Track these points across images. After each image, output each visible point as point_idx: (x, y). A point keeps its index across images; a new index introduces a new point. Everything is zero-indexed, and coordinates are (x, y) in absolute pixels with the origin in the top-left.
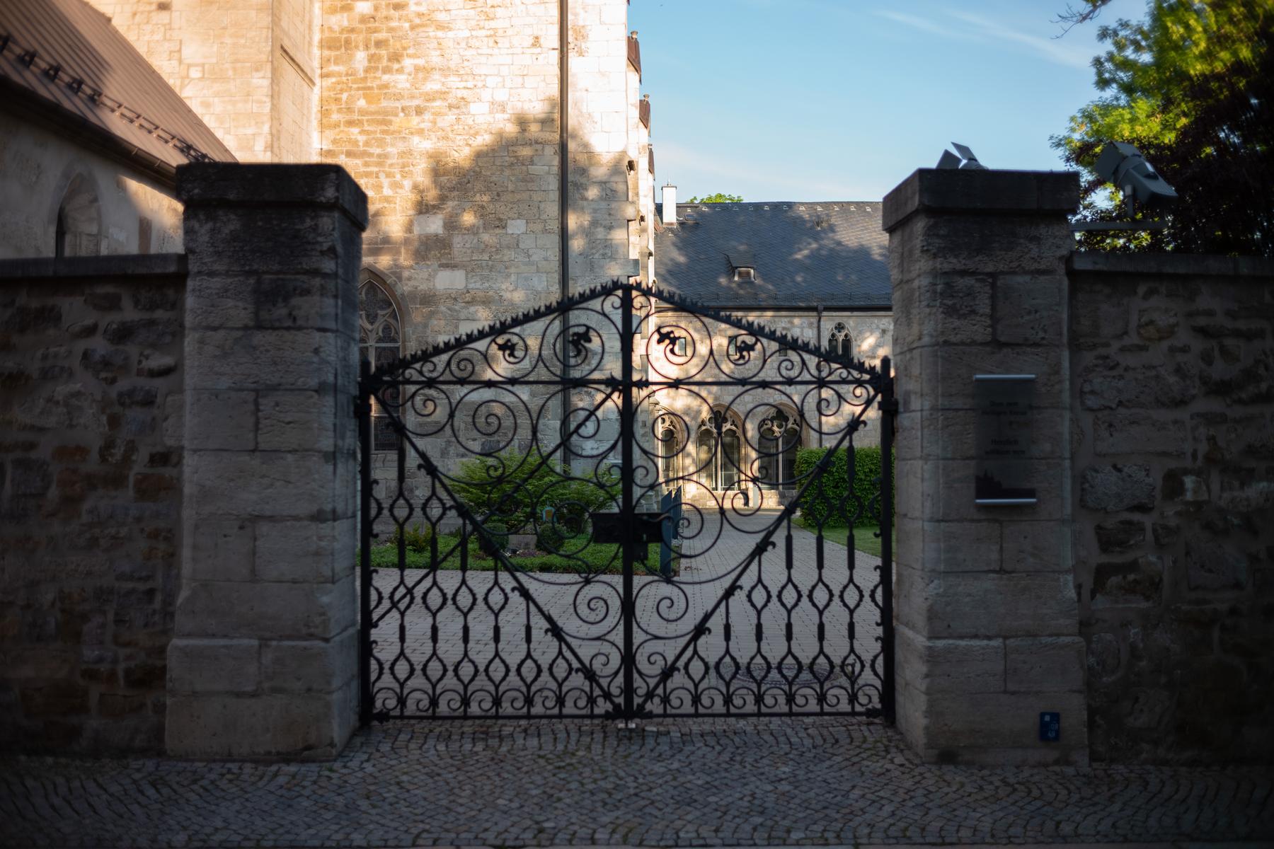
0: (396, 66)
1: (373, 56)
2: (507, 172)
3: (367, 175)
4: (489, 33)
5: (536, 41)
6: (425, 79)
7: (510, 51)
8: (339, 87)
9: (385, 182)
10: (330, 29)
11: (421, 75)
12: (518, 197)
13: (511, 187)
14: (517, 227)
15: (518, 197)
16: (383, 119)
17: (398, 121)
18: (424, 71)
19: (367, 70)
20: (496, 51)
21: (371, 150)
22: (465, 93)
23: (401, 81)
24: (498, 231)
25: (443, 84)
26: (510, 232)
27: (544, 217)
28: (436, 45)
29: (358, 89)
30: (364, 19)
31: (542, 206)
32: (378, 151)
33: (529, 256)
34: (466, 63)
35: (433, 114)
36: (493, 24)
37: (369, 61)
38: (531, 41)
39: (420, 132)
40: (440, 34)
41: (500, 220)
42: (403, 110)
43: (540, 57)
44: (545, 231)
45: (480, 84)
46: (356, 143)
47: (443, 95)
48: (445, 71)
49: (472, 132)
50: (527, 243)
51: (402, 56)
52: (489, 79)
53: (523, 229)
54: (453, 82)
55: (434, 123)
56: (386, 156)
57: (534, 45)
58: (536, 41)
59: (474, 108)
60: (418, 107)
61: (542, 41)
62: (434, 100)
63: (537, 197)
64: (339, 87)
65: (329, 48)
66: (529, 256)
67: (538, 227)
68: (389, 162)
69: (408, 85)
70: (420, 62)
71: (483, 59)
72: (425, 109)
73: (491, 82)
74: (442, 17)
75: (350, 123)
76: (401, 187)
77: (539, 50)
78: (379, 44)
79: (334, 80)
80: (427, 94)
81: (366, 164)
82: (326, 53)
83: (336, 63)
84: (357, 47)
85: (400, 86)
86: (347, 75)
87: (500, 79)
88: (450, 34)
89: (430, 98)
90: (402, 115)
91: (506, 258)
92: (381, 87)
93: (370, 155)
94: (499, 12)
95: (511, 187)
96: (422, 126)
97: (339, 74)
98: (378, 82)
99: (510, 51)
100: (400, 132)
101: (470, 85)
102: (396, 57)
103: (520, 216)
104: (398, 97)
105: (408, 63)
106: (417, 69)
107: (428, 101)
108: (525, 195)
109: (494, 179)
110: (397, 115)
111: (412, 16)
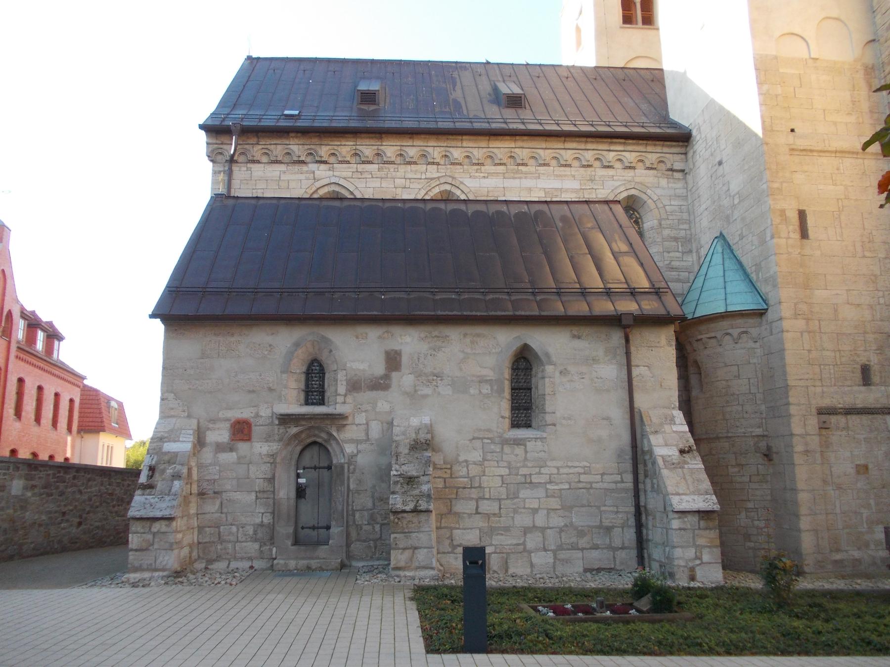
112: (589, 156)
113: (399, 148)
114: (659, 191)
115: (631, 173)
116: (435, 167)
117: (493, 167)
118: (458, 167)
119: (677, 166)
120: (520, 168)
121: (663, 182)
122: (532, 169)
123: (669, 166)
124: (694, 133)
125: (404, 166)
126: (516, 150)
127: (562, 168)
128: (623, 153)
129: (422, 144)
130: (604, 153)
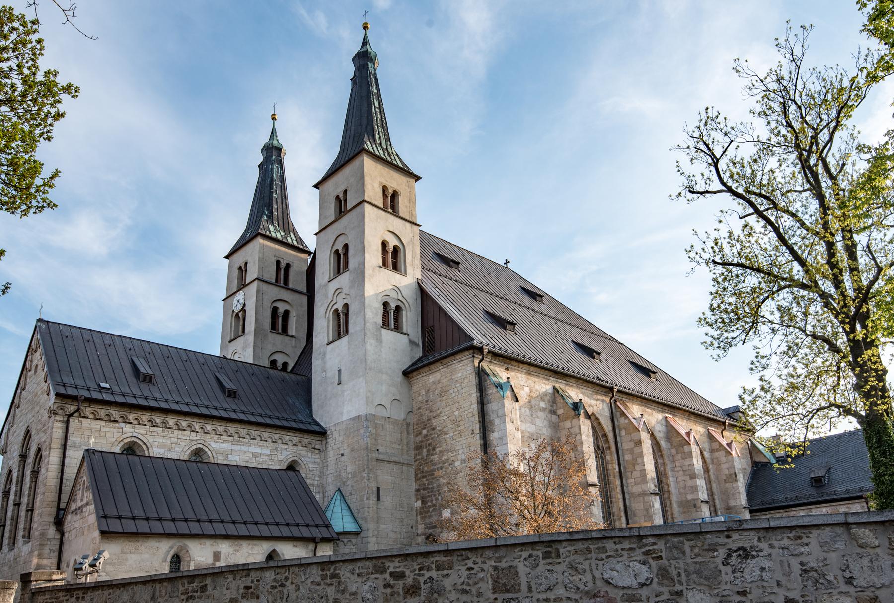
5: (473, 432)
9: (434, 498)
23: (436, 458)
46: (424, 484)
54: (450, 454)
58: (473, 432)
74: (445, 429)
75: (423, 477)
78: (429, 445)
94: (461, 423)
102: (434, 449)
105: (437, 450)
106: (440, 452)
112: (276, 436)
114: (307, 459)
115: (295, 448)
119: (317, 447)
121: (310, 454)
122: (247, 440)
124: (328, 433)
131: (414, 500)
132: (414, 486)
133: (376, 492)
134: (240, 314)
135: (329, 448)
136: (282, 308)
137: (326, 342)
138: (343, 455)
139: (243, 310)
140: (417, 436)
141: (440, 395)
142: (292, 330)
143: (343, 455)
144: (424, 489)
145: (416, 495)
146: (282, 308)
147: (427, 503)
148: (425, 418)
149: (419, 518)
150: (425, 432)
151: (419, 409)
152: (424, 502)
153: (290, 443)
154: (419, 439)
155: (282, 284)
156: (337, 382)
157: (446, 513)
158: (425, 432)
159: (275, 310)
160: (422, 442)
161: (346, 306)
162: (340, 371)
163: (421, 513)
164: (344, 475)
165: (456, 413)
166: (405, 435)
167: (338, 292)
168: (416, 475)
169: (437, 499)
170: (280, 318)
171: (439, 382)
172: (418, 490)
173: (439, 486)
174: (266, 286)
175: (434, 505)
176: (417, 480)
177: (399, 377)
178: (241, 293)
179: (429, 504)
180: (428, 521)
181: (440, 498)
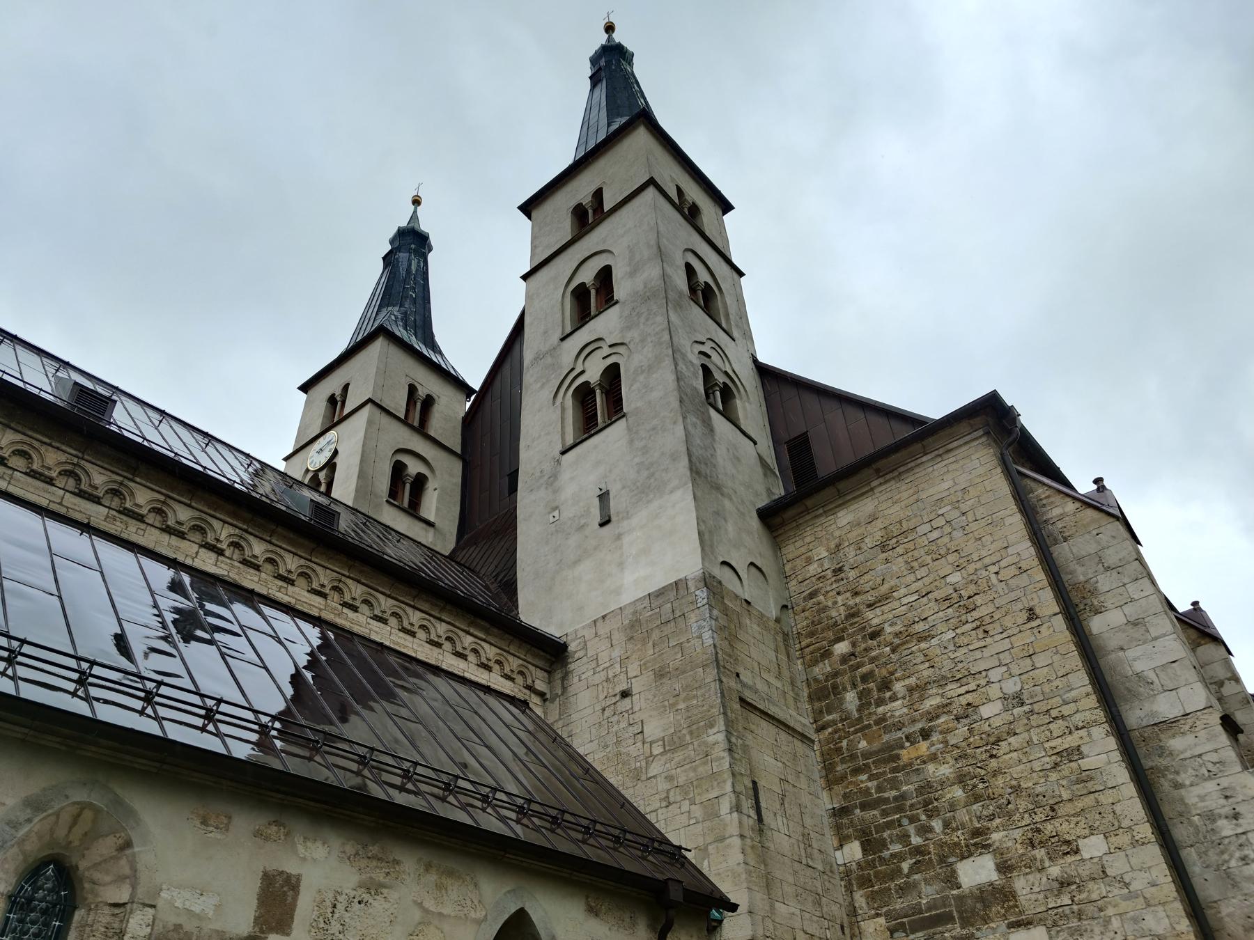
0: (888, 694)
1: (861, 692)
2: (1054, 776)
3: (888, 825)
4: (974, 625)
5: (1032, 614)
6: (922, 699)
7: (1005, 635)
8: (837, 736)
9: (911, 829)
10: (816, 680)
11: (916, 696)
12: (1080, 805)
13: (1065, 796)
14: (1093, 847)
15: (1080, 805)
16: (889, 754)
17: (906, 754)
18: (919, 691)
19: (859, 710)
20: (989, 640)
21: (886, 795)
22: (969, 698)
23: (897, 709)
24: (1069, 859)
25: (942, 695)
26: (1086, 855)
27: (1126, 823)
28: (923, 658)
29: (856, 732)
30: (844, 659)
31: (1118, 808)
32: (894, 793)
33: (1127, 885)
34: (960, 665)
35: (941, 733)
36: (975, 614)
37: (860, 699)
38: (1025, 615)
39: (933, 758)
40: (923, 645)
41: (1067, 842)
42: (908, 738)
43: (1043, 629)
44: (1135, 843)
45: (983, 682)
46: (867, 791)
47: (944, 708)
48: (942, 682)
49: (992, 739)
50: (1117, 866)
51: (891, 681)
52: (990, 673)
53: (1104, 848)
54: (953, 690)
55: (946, 742)
56: (903, 797)
57: (1029, 619)
58: (1032, 614)
59: (986, 711)
60: (922, 730)
61: (1037, 611)
62: (938, 717)
63: (1106, 798)
64: (837, 736)
65: (819, 699)
66: (1127, 885)
67: (1124, 839)
68: (908, 803)
69: (905, 710)
70: (912, 681)
71: (978, 654)
72: (931, 729)
73: (994, 675)
74: (920, 627)
75: (857, 771)
76: (931, 830)
77: (1038, 622)
78: (865, 678)
79: (830, 730)
80: (929, 713)
81: (885, 813)
82: (817, 705)
83: (829, 713)
84: (845, 689)
85: (897, 714)
86: (842, 720)
87: (1005, 669)
88: (934, 641)
89: (932, 716)
90: (907, 744)
91: (1095, 896)
92: (877, 723)
93: (886, 801)
94: (979, 600)
95: (1065, 796)
96: (933, 749)
97: (834, 722)
98: (875, 717)
99: (1005, 635)
100: (911, 764)
101: (972, 686)
102: (885, 685)
103: (1093, 830)
104: (899, 726)
105: (898, 687)
106: (911, 690)
107: (931, 720)
108: (1089, 801)
109: (1039, 789)
110: (902, 747)
111: (889, 638)
113: (162, 498)
116: (213, 556)
117: (306, 594)
118: (252, 571)
119: (540, 686)
120: (345, 610)
123: (529, 682)
124: (572, 648)
125: (157, 532)
126: (349, 581)
127: (401, 634)
128: (483, 644)
129: (206, 509)
130: (461, 633)
131: (831, 840)
132: (827, 801)
133: (751, 792)
134: (322, 476)
135: (575, 684)
136: (414, 467)
137: (559, 448)
138: (625, 694)
139: (331, 465)
140: (815, 662)
141: (883, 547)
142: (431, 505)
143: (625, 694)
144: (864, 807)
145: (838, 828)
146: (414, 467)
147: (883, 845)
148: (838, 613)
149: (860, 899)
150: (842, 648)
151: (812, 595)
152: (870, 845)
153: (472, 657)
154: (822, 669)
155: (416, 424)
156: (597, 519)
157: (977, 872)
158: (842, 648)
159: (398, 470)
160: (836, 674)
161: (613, 373)
162: (604, 497)
163: (865, 882)
164: (634, 750)
165: (955, 578)
166: (783, 657)
167: (587, 350)
168: (828, 768)
169: (925, 830)
170: (408, 487)
171: (872, 519)
172: (840, 813)
173: (926, 788)
174: (385, 420)
175: (918, 851)
176: (831, 779)
177: (755, 523)
178: (332, 434)
179: (896, 848)
180: (898, 905)
181: (937, 825)
